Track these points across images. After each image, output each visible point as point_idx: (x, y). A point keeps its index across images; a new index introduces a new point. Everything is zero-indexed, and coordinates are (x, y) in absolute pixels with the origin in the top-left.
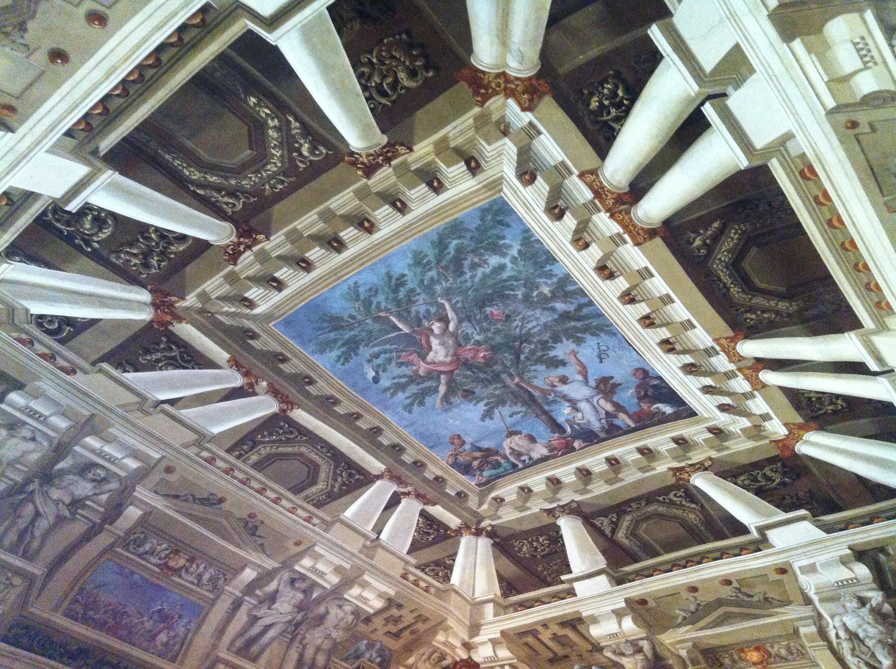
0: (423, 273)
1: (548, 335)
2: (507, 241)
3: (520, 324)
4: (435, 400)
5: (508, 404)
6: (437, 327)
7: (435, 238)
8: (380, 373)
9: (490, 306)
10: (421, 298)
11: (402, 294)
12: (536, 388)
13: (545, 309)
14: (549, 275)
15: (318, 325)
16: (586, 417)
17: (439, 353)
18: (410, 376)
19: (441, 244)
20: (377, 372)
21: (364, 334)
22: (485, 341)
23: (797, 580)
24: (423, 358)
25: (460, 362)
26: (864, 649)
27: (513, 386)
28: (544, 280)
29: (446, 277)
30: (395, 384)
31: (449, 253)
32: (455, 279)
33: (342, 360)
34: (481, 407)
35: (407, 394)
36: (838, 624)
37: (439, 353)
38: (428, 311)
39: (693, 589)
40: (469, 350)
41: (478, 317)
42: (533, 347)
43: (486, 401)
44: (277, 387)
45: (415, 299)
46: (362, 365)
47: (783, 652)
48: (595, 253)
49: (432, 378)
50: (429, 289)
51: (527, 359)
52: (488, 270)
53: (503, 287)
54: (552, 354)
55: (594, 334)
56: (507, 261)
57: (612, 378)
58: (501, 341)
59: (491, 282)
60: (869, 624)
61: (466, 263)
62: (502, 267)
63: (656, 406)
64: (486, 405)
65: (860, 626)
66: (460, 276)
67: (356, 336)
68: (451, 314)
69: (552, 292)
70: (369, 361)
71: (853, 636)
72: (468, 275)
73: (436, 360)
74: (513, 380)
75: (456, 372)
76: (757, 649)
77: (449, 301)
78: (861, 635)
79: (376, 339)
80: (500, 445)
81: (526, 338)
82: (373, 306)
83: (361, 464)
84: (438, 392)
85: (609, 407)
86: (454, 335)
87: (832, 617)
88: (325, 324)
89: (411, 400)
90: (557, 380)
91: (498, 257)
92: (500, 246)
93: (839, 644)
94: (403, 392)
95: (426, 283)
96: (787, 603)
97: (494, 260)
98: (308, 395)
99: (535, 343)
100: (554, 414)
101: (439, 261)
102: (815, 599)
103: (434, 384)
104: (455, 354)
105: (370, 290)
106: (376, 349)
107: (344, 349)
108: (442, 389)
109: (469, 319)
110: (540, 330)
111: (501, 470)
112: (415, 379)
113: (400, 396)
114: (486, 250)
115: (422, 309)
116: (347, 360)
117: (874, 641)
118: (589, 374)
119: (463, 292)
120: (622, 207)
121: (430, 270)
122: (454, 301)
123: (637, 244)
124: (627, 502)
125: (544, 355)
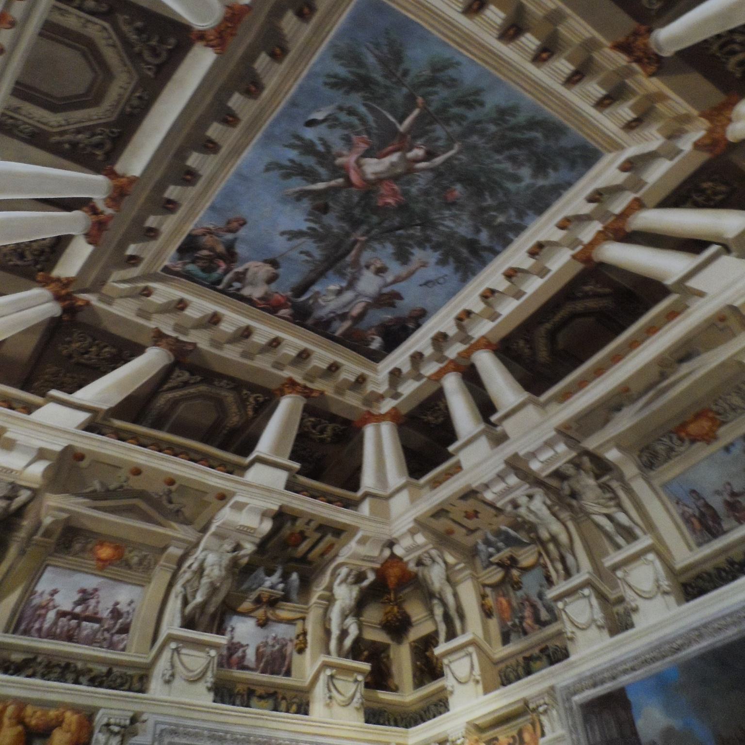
0: (494, 121)
1: (441, 239)
4: (298, 184)
5: (323, 244)
10: (455, 128)
11: (455, 110)
12: (358, 256)
14: (521, 214)
17: (373, 167)
19: (534, 124)
23: (219, 510)
24: (367, 154)
25: (371, 187)
26: (196, 584)
33: (333, 80)
34: (304, 226)
36: (201, 557)
37: (373, 167)
38: (438, 139)
39: (137, 471)
40: (393, 189)
41: (445, 182)
44: (247, 18)
47: (135, 560)
48: (558, 235)
50: (471, 130)
51: (400, 236)
52: (511, 171)
55: (457, 269)
60: (220, 566)
61: (515, 151)
62: (517, 179)
64: (310, 228)
65: (212, 565)
68: (438, 160)
69: (501, 225)
71: (200, 571)
74: (363, 235)
76: (117, 548)
78: (206, 572)
81: (427, 223)
82: (430, 89)
83: (130, 148)
84: (314, 182)
85: (356, 311)
86: (410, 171)
87: (204, 549)
88: (385, 49)
90: (378, 265)
93: (185, 572)
95: (478, 126)
96: (187, 522)
97: (525, 172)
98: (250, 57)
100: (322, 280)
101: (512, 129)
102: (213, 529)
103: (324, 177)
106: (363, 110)
108: (320, 186)
110: (443, 231)
112: (326, 157)
113: (293, 154)
117: (209, 580)
120: (611, 235)
121: (497, 124)
122: (461, 156)
123: (574, 257)
124: (221, 376)
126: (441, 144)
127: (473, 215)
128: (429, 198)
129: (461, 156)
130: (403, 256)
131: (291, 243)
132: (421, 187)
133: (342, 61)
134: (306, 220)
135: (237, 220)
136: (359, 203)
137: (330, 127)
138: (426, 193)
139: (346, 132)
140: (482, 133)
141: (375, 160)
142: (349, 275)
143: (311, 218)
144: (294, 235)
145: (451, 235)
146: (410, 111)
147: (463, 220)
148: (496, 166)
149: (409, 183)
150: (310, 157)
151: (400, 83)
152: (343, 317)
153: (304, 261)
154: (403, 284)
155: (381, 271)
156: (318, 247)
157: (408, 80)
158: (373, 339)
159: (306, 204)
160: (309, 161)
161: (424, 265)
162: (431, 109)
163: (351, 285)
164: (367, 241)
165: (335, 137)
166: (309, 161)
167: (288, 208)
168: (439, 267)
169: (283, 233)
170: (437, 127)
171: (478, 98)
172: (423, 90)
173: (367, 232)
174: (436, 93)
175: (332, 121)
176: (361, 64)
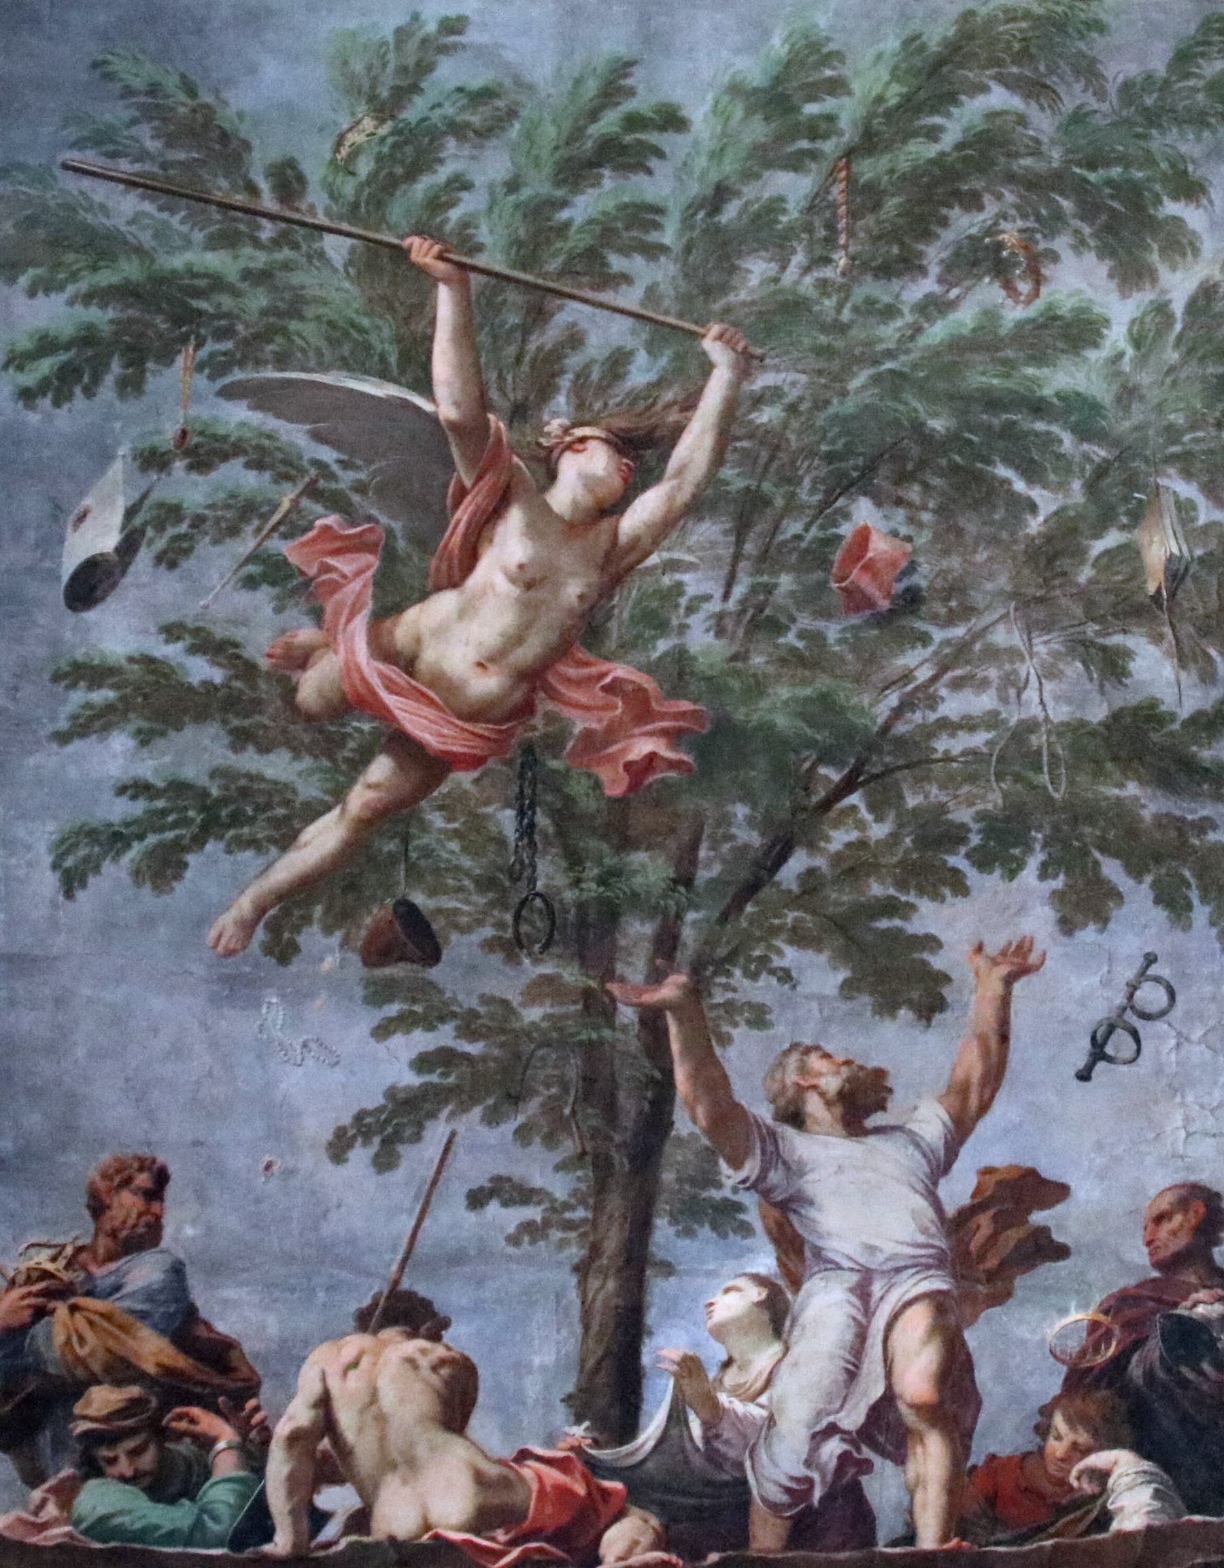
0: (764, 158)
1: (993, 800)
2: (1193, 217)
3: (924, 674)
4: (232, 885)
6: (585, 469)
7: (937, 34)
8: (144, 558)
9: (879, 504)
10: (648, 277)
11: (584, 207)
12: (714, 1082)
13: (1083, 648)
15: (114, 113)
16: (786, 1384)
17: (467, 630)
18: (248, 670)
19: (935, 76)
20: (129, 546)
21: (258, 300)
22: (714, 686)
24: (393, 596)
25: (517, 726)
27: (627, 1014)
28: (1187, 490)
29: (830, 241)
30: (148, 661)
31: (933, 134)
32: (860, 267)
33: (46, 366)
34: (395, 1064)
35: (148, 768)
37: (467, 630)
38: (618, 362)
41: (793, 527)
42: (879, 831)
43: (445, 1036)
45: (617, 263)
46: (105, 457)
49: (328, 746)
50: (715, 252)
52: (1014, 314)
53: (1009, 431)
54: (930, 916)
55: (1172, 900)
56: (1121, 313)
57: (1060, 1192)
58: (782, 721)
59: (981, 377)
61: (964, 224)
62: (1079, 331)
63: (1099, 1459)
64: (422, 1063)
66: (885, 271)
67: (217, 283)
69: (1176, 574)
70: (152, 460)
72: (927, 285)
73: (429, 656)
74: (656, 977)
75: (463, 779)
77: (746, 364)
79: (282, 361)
80: (292, 1356)
81: (877, 762)
82: (422, 187)
84: (286, 839)
85: (917, 1373)
86: (617, 565)
89: (138, 808)
90: (832, 1083)
91: (1102, 269)
92: (1153, 225)
94: (145, 739)
95: (730, 213)
97: (1077, 278)
99: (906, 819)
100: (659, 1289)
101: (869, 142)
103: (309, 790)
104: (534, 679)
105: (485, 95)
106: (238, 416)
107: (101, 317)
108: (322, 838)
109: (747, 511)
111: (178, 1516)
112: (251, 698)
113: (116, 755)
114: (1088, 210)
115: (604, 333)
116: (61, 386)
118: (984, 1128)
119: (834, 365)
121: (795, 163)
122: (763, 381)
125: (890, 907)
126: (652, 377)
127: (1035, 610)
128: (790, 638)
129: (763, 381)
130: (902, 980)
131: (399, 1175)
132: (715, 606)
133: (23, 281)
134: (383, 1031)
135: (120, 1176)
136: (527, 830)
137: (169, 559)
138: (760, 620)
139: (246, 544)
140: (765, 229)
141: (445, 603)
142: (750, 1200)
143: (393, 1009)
144: (387, 1128)
145: (1016, 750)
146: (423, 309)
147: (1013, 654)
148: (937, 332)
149: (654, 620)
150: (189, 732)
151: (299, 231)
152: (885, 1430)
153: (514, 1240)
154: (1003, 1110)
155: (862, 1102)
156: (523, 1134)
157: (316, 202)
158: (1101, 1476)
159: (326, 952)
160: (200, 753)
161: (1020, 963)
162: (493, 259)
163: (796, 1250)
164: (697, 991)
165: (213, 583)
166: (200, 753)
167: (274, 1010)
168: (1088, 934)
169: (339, 1148)
170: (570, 313)
171: (630, 106)
172: (397, 211)
173: (666, 944)
174: (460, 184)
175: (162, 532)
176: (102, 246)
